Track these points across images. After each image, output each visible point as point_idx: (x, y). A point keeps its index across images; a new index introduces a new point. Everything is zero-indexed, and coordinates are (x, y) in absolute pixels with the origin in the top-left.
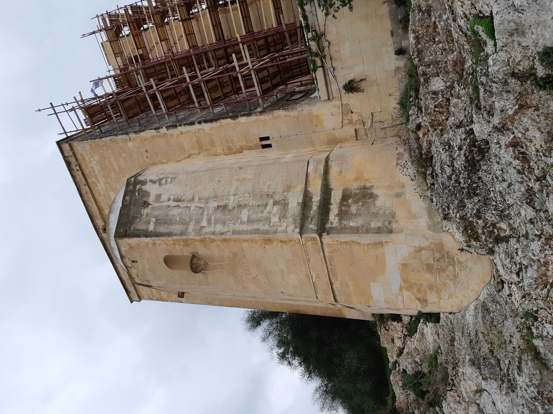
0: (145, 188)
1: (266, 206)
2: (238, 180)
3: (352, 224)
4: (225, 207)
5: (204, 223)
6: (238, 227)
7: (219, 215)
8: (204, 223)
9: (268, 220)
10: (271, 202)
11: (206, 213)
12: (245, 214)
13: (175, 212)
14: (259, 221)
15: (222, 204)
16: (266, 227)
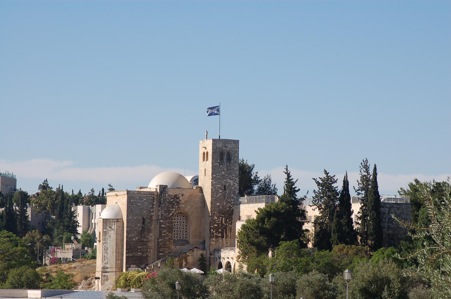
0: (113, 225)
1: (107, 259)
2: (113, 252)
3: (103, 278)
4: (108, 249)
5: (105, 245)
6: (103, 253)
7: (106, 248)
8: (105, 245)
9: (105, 260)
10: (108, 260)
11: (107, 245)
12: (106, 255)
13: (107, 236)
14: (105, 258)
15: (108, 249)
16: (103, 260)
